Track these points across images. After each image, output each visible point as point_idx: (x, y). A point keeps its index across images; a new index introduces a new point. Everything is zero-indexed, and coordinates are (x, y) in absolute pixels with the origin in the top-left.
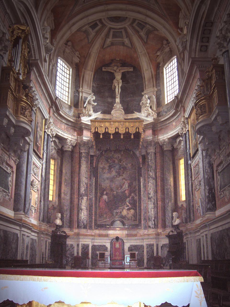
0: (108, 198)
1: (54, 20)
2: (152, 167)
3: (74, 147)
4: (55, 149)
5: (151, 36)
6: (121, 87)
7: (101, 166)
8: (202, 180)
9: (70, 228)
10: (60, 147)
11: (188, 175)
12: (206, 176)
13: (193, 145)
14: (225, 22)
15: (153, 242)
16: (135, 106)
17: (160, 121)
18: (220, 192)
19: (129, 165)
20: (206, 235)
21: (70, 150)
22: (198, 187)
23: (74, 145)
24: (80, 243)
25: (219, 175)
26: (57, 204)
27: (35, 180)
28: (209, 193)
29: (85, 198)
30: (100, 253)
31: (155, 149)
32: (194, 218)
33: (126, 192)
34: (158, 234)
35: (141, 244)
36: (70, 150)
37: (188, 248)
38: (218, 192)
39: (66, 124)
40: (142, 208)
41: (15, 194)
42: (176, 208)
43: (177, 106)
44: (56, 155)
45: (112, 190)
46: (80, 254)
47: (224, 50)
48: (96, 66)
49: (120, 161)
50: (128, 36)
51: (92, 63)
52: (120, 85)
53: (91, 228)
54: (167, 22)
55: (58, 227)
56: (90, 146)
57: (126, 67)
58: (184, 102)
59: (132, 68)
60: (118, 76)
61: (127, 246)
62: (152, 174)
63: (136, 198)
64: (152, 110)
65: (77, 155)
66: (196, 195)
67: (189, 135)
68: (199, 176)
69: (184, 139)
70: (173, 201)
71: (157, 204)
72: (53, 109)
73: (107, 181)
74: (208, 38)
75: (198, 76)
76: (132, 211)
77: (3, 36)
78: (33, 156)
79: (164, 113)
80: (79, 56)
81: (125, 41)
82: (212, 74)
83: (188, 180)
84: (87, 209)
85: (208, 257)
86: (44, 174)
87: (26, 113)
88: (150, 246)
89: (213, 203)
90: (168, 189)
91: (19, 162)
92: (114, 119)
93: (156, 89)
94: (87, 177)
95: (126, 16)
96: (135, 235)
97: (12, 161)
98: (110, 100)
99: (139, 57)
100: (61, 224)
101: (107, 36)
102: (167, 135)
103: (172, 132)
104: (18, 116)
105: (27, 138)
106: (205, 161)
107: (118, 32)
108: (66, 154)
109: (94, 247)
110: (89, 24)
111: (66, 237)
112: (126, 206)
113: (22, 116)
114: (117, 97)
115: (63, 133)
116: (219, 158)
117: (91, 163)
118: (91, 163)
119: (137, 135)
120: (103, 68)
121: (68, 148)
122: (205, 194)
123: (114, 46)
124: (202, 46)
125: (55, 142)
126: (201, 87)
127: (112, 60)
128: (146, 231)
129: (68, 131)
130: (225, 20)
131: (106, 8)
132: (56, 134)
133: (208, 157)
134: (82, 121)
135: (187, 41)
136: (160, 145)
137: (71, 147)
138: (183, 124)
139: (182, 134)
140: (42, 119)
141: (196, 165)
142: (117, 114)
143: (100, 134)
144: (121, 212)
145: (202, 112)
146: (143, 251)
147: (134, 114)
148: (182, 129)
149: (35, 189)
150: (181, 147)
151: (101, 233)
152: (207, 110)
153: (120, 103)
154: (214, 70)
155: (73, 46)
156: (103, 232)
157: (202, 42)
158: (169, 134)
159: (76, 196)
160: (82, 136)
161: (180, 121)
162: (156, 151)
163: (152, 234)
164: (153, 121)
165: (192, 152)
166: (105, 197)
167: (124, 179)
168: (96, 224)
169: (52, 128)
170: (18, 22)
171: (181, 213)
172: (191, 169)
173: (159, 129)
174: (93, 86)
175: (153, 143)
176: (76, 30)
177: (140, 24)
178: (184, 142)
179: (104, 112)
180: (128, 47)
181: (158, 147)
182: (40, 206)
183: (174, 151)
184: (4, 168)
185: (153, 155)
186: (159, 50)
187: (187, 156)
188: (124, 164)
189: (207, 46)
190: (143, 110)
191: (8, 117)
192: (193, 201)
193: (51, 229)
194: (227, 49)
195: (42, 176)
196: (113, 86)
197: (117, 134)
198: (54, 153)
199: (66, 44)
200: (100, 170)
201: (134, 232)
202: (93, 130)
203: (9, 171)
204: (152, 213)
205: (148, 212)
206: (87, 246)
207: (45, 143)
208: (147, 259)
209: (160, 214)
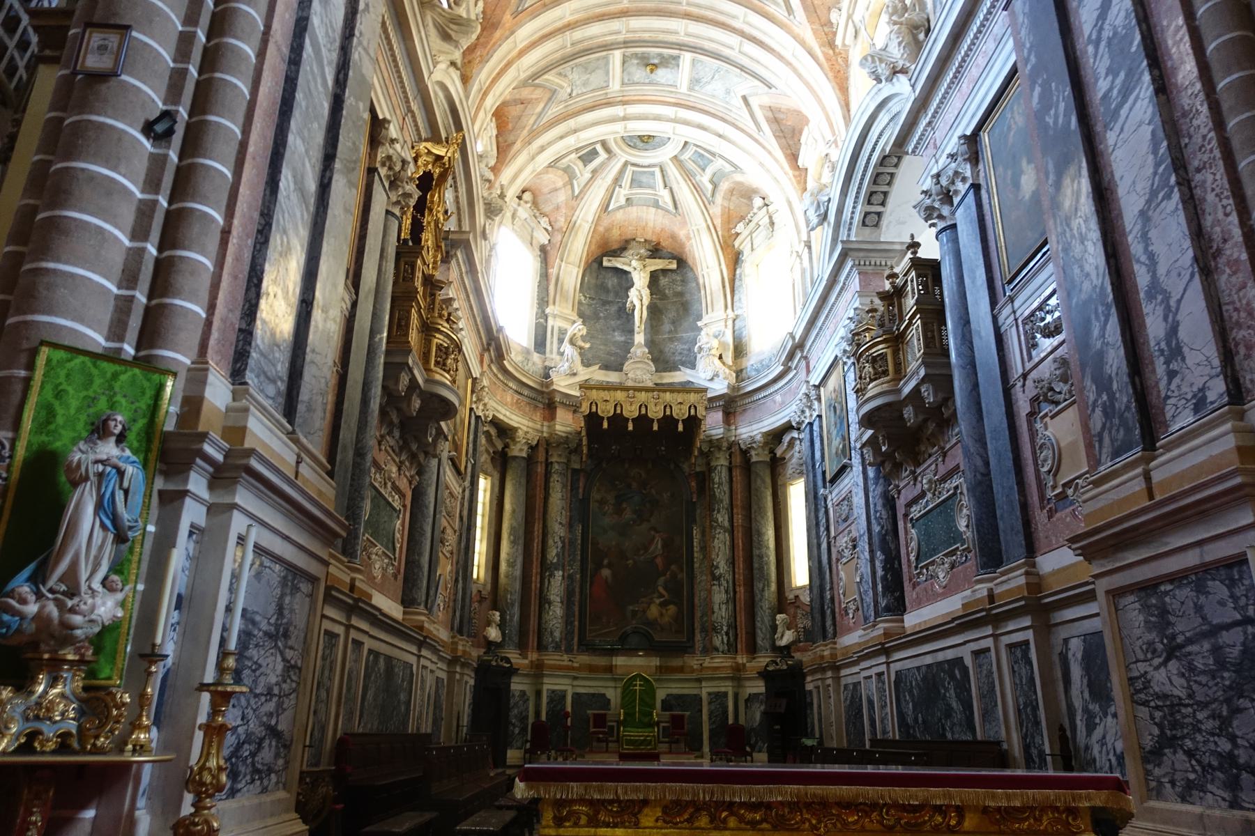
1: (497, 136)
2: (722, 501)
3: (533, 448)
4: (487, 451)
5: (724, 186)
6: (648, 308)
7: (595, 495)
8: (861, 536)
9: (520, 649)
10: (500, 446)
11: (817, 524)
12: (876, 528)
13: (834, 451)
14: (952, 156)
15: (727, 687)
16: (681, 353)
17: (742, 392)
18: (916, 568)
19: (666, 496)
20: (880, 675)
21: (524, 455)
22: (847, 553)
23: (535, 443)
24: (545, 687)
25: (913, 527)
26: (489, 587)
27: (448, 527)
28: (884, 568)
29: (559, 574)
30: (594, 714)
31: (730, 456)
32: (835, 630)
33: (659, 561)
35: (695, 692)
36: (524, 455)
37: (819, 707)
38: (909, 566)
39: (516, 391)
40: (696, 600)
41: (406, 564)
43: (791, 356)
44: (489, 467)
46: (544, 718)
47: (941, 225)
48: (588, 255)
51: (579, 247)
52: (646, 301)
53: (569, 650)
54: (770, 153)
55: (490, 645)
56: (573, 445)
57: (660, 258)
58: (809, 349)
59: (675, 261)
60: (640, 280)
61: (661, 694)
62: (722, 518)
63: (683, 576)
64: (724, 363)
65: (540, 469)
66: (842, 574)
67: (821, 427)
68: (853, 527)
69: (805, 435)
70: (773, 587)
71: (735, 592)
72: (490, 356)
74: (885, 194)
75: (855, 284)
76: (672, 609)
77: (403, 168)
78: (447, 469)
79: (754, 373)
80: (550, 229)
81: (661, 196)
82: (907, 281)
83: (818, 537)
84: (562, 602)
85: (884, 732)
86: (465, 513)
87: (449, 361)
88: (719, 697)
89: (897, 594)
90: (761, 557)
91: (419, 483)
92: (630, 384)
93: (731, 314)
94: (564, 522)
95: (667, 136)
96: (681, 670)
97: (405, 480)
98: (619, 337)
99: (692, 236)
100: (499, 640)
102: (761, 425)
103: (773, 419)
104: (431, 370)
105: (443, 424)
106: (874, 490)
107: (645, 172)
108: (514, 464)
109: (577, 696)
110: (577, 150)
111: (512, 671)
112: (655, 595)
113: (439, 370)
114: (636, 329)
115: (508, 413)
116: (915, 484)
117: (574, 488)
118: (572, 490)
119: (693, 422)
120: (605, 259)
121: (518, 450)
122: (874, 573)
123: (635, 208)
124: (867, 214)
125: (487, 434)
126: (868, 312)
127: (627, 242)
128: (708, 660)
129: (519, 409)
130: (948, 151)
131: (622, 114)
132: (494, 416)
133: (881, 481)
134: (555, 387)
135: (829, 200)
136: (741, 449)
137: (525, 448)
138: (804, 401)
139: (798, 423)
140: (467, 379)
141: (843, 500)
142: (639, 372)
143: (603, 418)
144: (644, 612)
145: (875, 374)
146: (701, 711)
147: (678, 373)
148: (803, 412)
149: (446, 550)
150: (793, 455)
151: (593, 663)
152: (891, 368)
153: (646, 345)
154: (914, 273)
155: (535, 203)
156: (601, 661)
157: (869, 203)
158: (766, 423)
159: (535, 569)
160: (552, 423)
161: (796, 394)
162: (730, 463)
163: (724, 667)
164: (725, 391)
165: (831, 469)
166: (606, 572)
167: (654, 529)
168: (580, 643)
169: (486, 400)
170: (435, 138)
171: (795, 617)
172: (826, 507)
173: (739, 409)
174: (580, 303)
175: (725, 444)
176: (546, 164)
177: (701, 156)
178: (808, 444)
179: (606, 367)
180: (667, 211)
181: (738, 452)
182: (456, 594)
183: (776, 465)
184: (387, 496)
185: (725, 474)
186: (742, 218)
187: (815, 476)
188: (653, 492)
189: (879, 214)
190: (701, 364)
191: (411, 370)
192: (832, 588)
193: (475, 653)
194: (949, 223)
195: (461, 518)
196: (628, 305)
197: (642, 420)
198: (485, 462)
199: (520, 198)
200: (593, 506)
201: (676, 662)
202: (585, 409)
203: (396, 505)
204: (722, 614)
205: (713, 612)
206: (563, 695)
207: (471, 437)
208: (711, 731)
209: (742, 618)
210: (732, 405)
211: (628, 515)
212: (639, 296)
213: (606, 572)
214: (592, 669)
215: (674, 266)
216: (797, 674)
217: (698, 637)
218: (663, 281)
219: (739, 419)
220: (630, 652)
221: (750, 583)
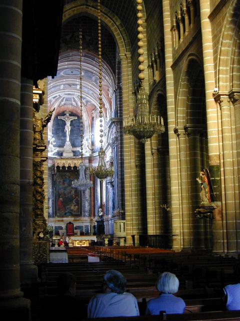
0: (63, 199)
6: (70, 131)
15: (89, 224)
34: (91, 220)
42: (102, 206)
45: (65, 194)
49: (69, 177)
50: (75, 101)
53: (53, 217)
60: (68, 124)
63: (79, 199)
73: (62, 190)
75: (110, 150)
76: (77, 207)
88: (87, 226)
93: (91, 134)
96: (78, 220)
98: (63, 138)
101: (62, 101)
117: (53, 179)
127: (64, 112)
144: (70, 208)
166: (61, 199)
186: (94, 109)
200: (58, 183)
201: (78, 219)
210: (90, 159)
211: (66, 185)
212: (68, 128)
213: (61, 199)
214: (59, 221)
215: (77, 118)
216: (102, 221)
217: (83, 213)
218: (74, 122)
219: (93, 162)
220: (67, 217)
221: (94, 201)
